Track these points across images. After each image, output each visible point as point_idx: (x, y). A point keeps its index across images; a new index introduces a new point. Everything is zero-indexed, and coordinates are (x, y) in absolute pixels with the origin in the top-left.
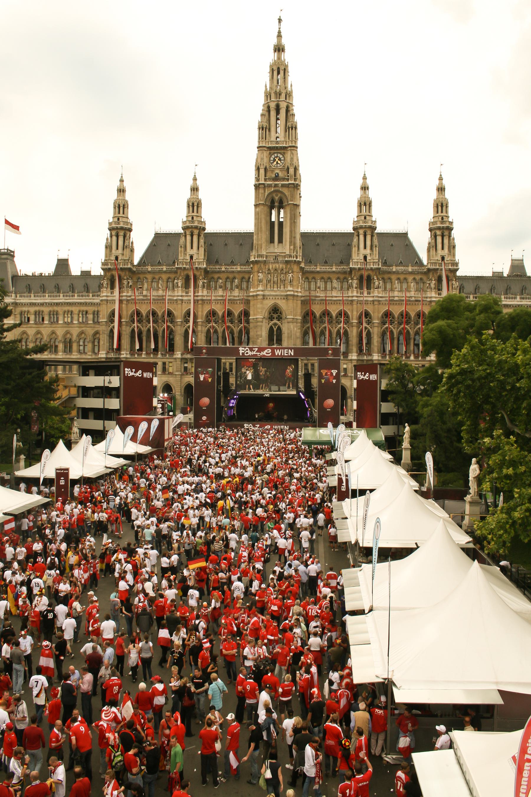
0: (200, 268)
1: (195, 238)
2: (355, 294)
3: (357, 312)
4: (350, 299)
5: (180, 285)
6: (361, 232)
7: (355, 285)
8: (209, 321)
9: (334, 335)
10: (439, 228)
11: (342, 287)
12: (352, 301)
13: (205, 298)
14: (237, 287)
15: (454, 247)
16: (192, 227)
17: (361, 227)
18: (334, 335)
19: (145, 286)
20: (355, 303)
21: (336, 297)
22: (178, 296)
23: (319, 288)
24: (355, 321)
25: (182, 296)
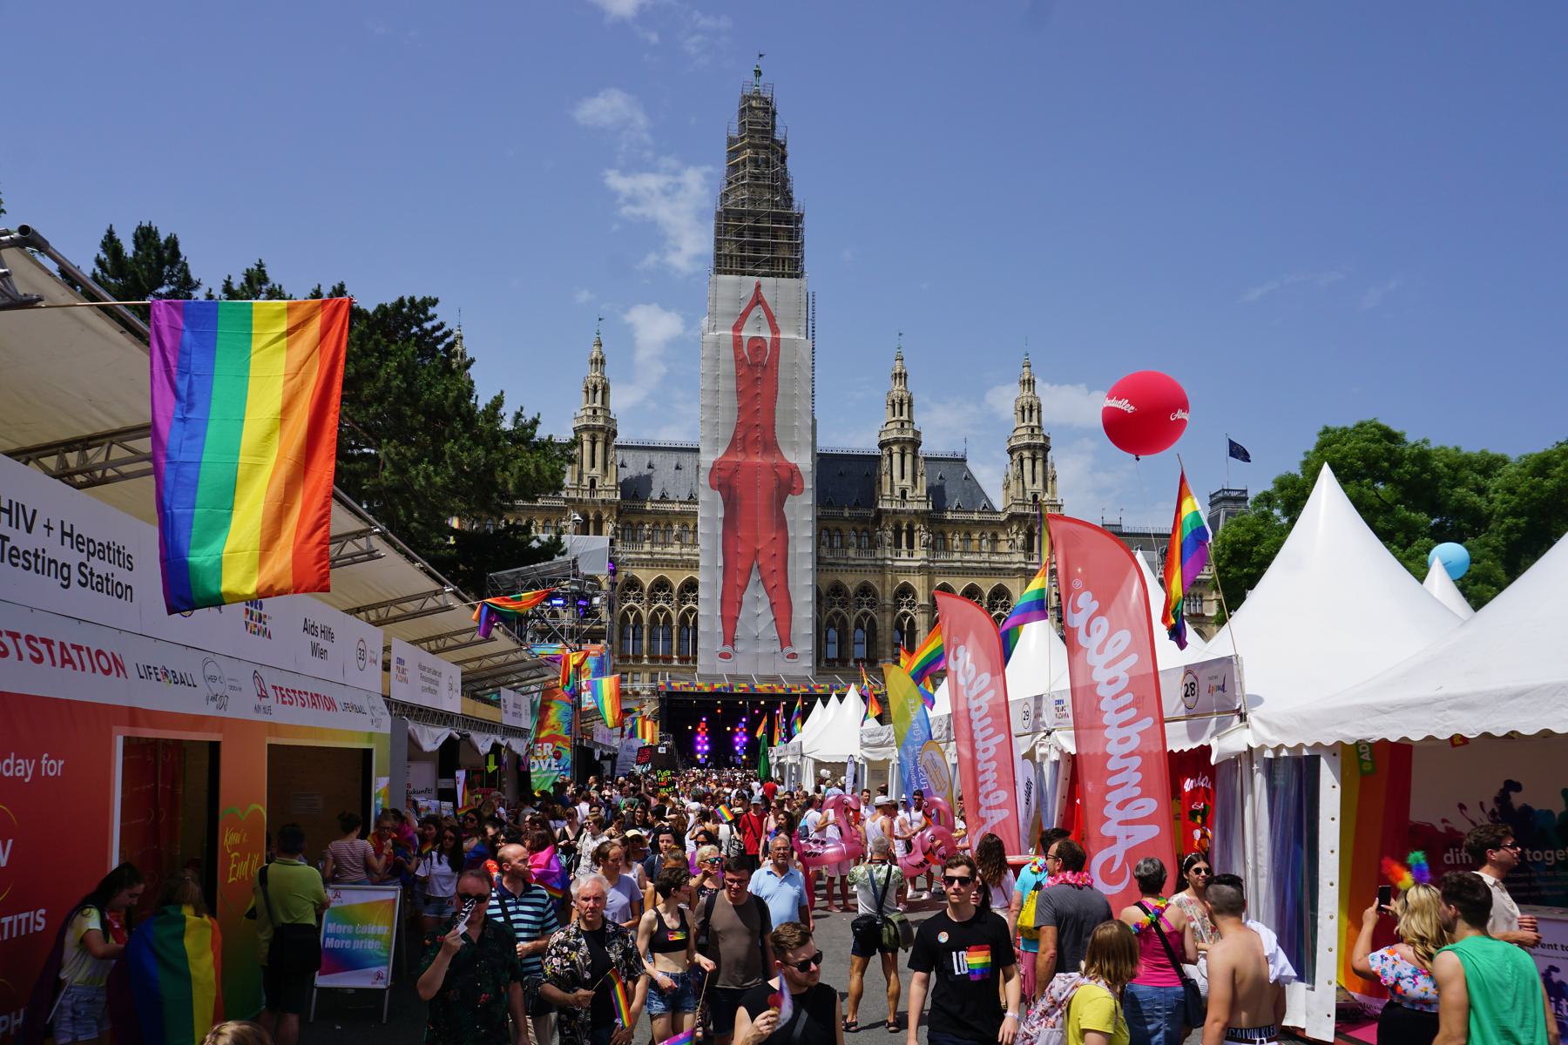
0: (610, 502)
1: (599, 447)
6: (895, 448)
7: (887, 540)
10: (1028, 447)
11: (859, 547)
12: (883, 567)
14: (679, 537)
15: (1054, 479)
17: (896, 441)
24: (889, 601)
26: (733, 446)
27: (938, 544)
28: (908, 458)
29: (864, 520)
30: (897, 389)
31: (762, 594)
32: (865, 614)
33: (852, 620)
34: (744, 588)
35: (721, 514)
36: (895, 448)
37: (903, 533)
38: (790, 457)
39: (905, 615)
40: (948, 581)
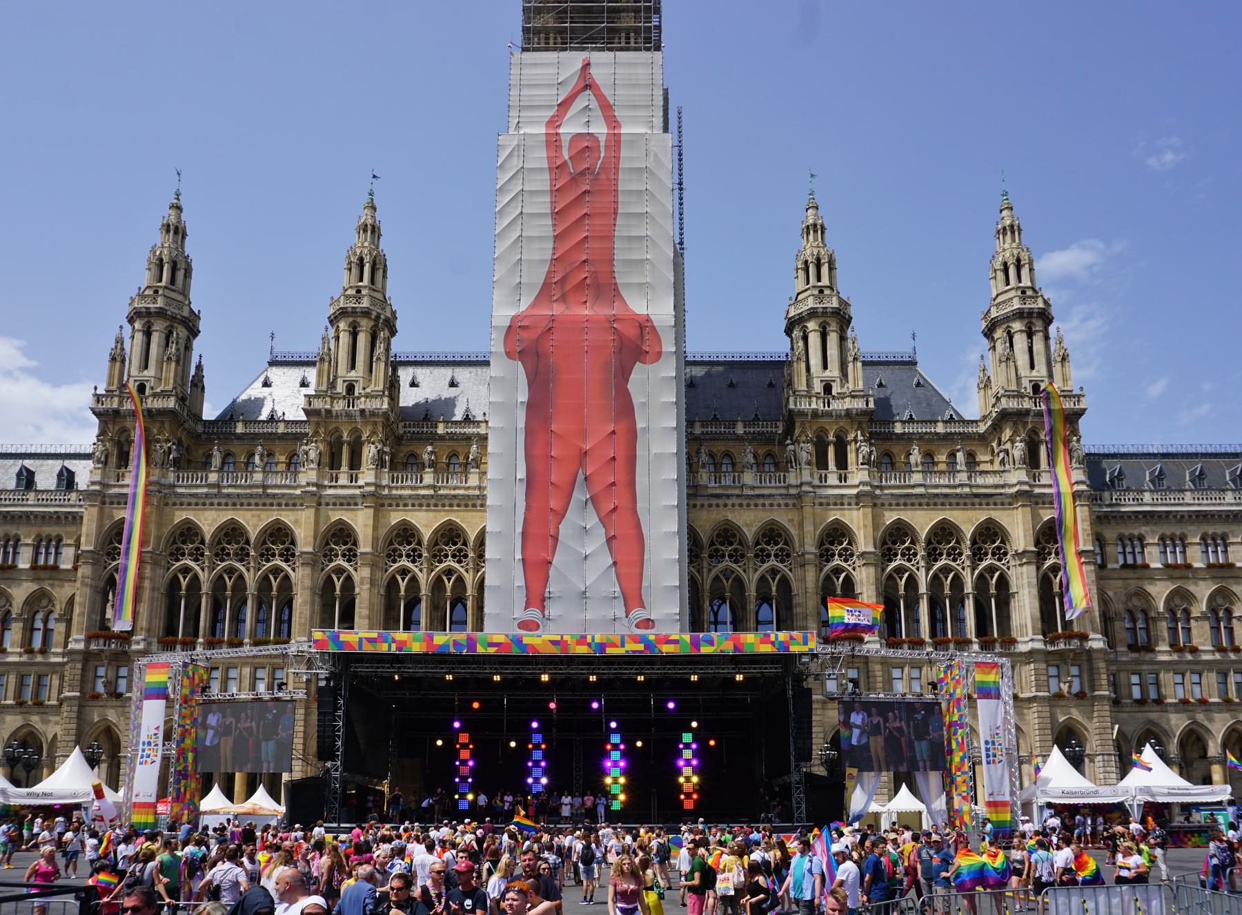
0: (373, 413)
1: (363, 339)
2: (806, 477)
3: (815, 525)
4: (793, 491)
5: (312, 455)
6: (812, 325)
7: (804, 456)
8: (393, 556)
9: (752, 591)
12: (799, 497)
13: (386, 492)
16: (354, 312)
17: (813, 314)
18: (752, 591)
19: (217, 460)
20: (807, 501)
21: (753, 488)
22: (308, 484)
23: (704, 466)
24: (811, 548)
25: (317, 485)
26: (545, 292)
27: (886, 460)
28: (833, 339)
29: (768, 439)
30: (809, 248)
31: (592, 521)
32: (774, 571)
33: (751, 580)
34: (561, 515)
35: (523, 396)
36: (812, 325)
37: (830, 449)
38: (638, 306)
39: (837, 571)
40: (907, 516)
